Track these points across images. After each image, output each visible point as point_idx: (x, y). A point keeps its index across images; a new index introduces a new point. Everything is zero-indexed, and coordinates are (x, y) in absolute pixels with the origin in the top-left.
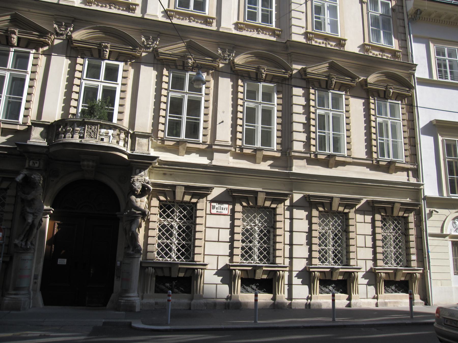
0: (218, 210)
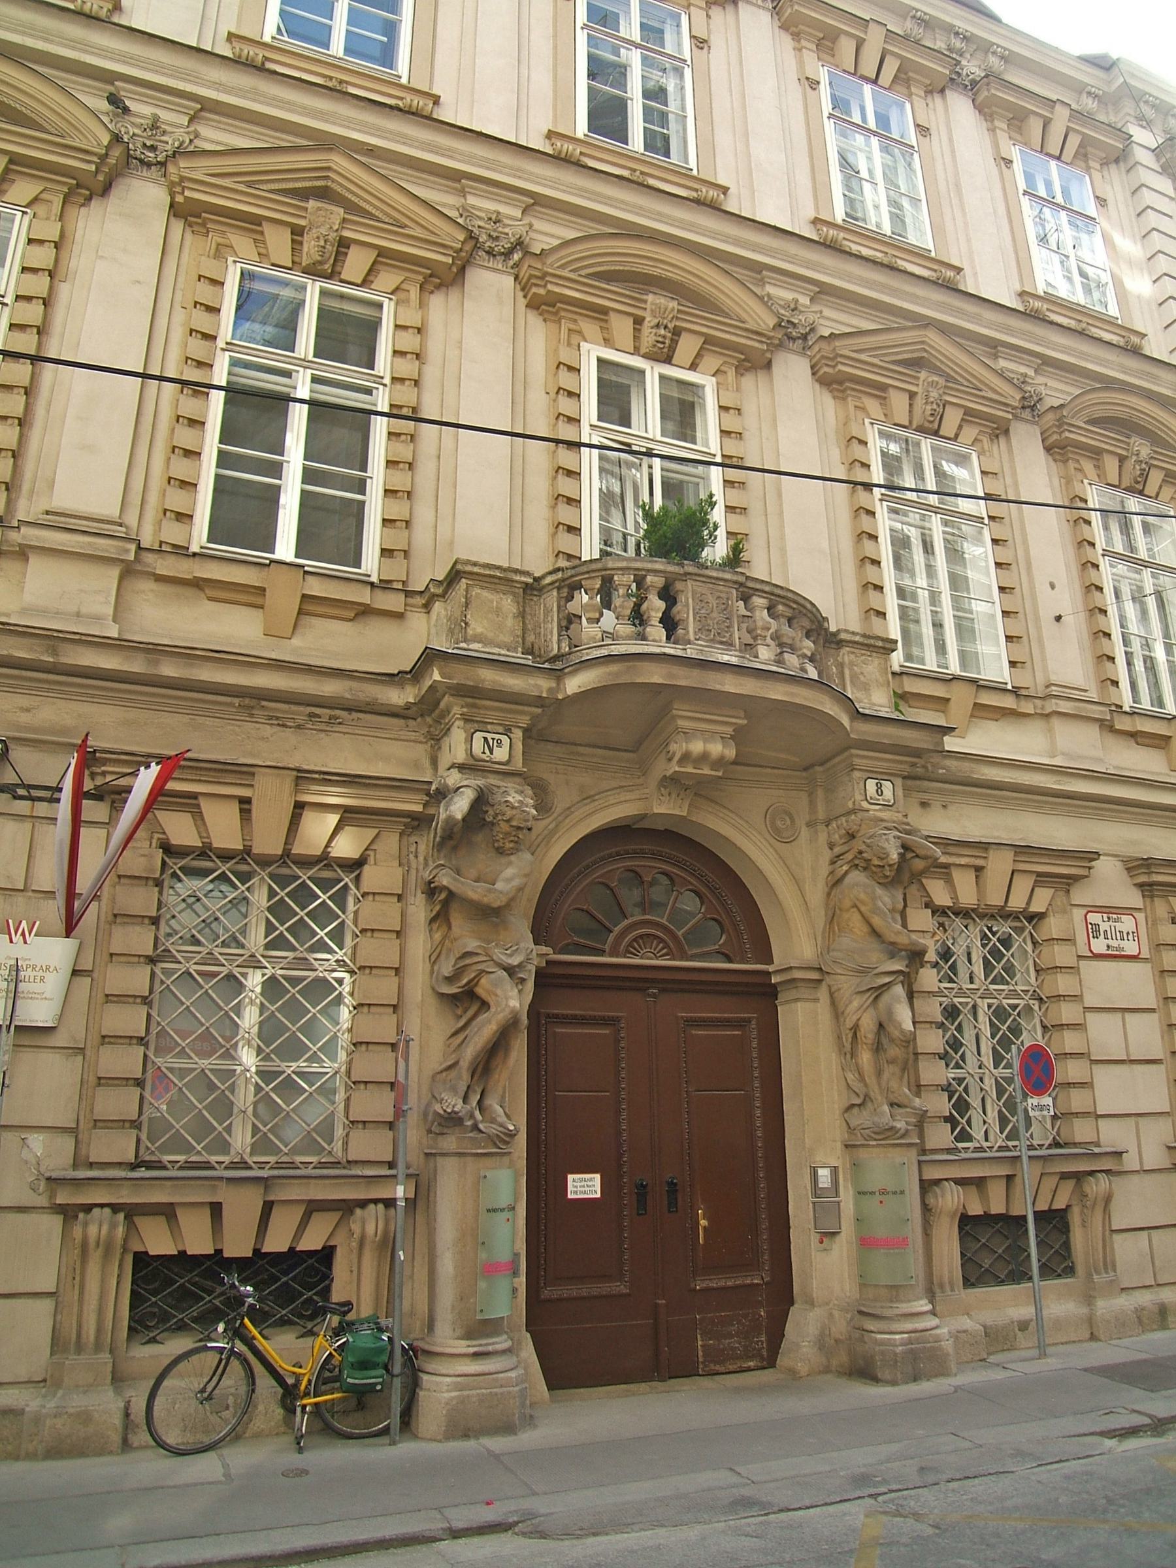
0: (1110, 942)
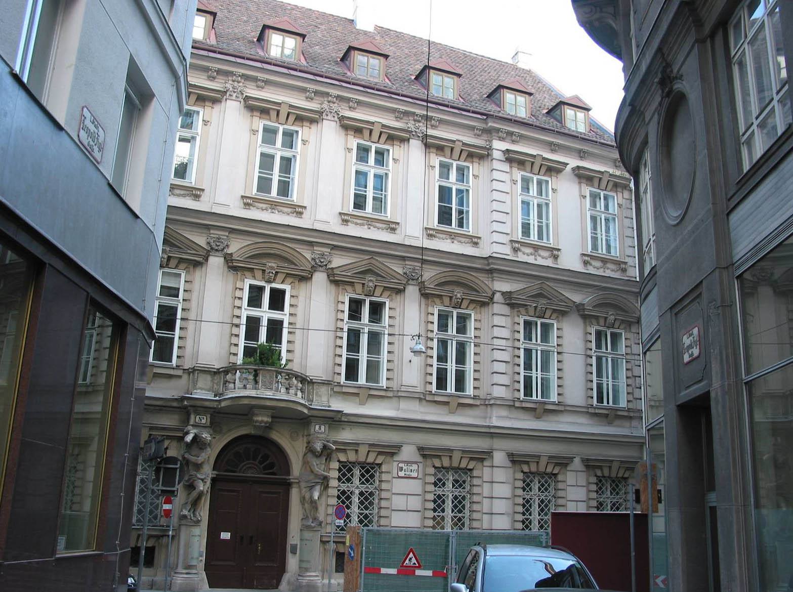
0: (406, 473)
